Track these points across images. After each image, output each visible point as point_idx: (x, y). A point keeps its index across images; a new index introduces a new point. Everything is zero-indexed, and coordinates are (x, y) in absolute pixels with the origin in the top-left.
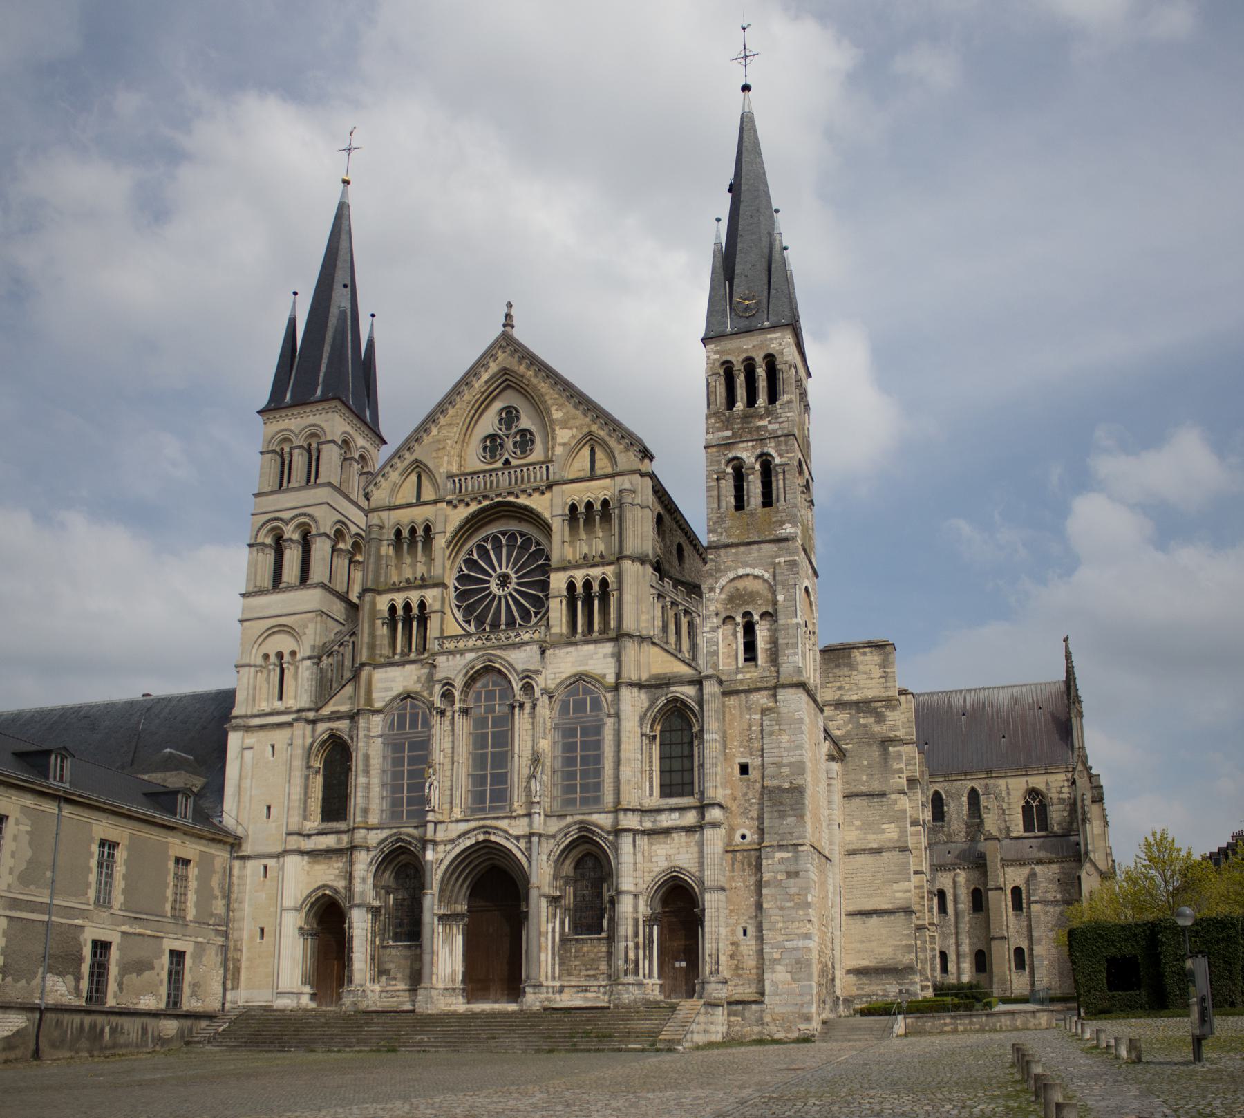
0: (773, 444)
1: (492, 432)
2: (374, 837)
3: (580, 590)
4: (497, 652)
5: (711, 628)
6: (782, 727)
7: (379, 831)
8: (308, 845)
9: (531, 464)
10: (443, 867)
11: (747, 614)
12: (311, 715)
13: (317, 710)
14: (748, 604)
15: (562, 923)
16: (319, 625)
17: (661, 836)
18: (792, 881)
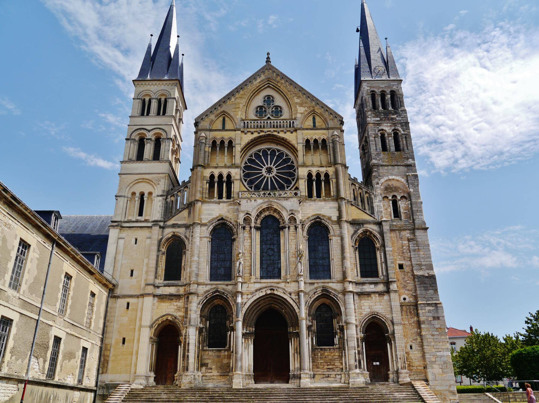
0: (399, 126)
1: (261, 104)
2: (202, 290)
3: (314, 178)
4: (275, 200)
5: (379, 200)
6: (419, 248)
7: (204, 286)
8: (159, 291)
9: (282, 120)
10: (246, 306)
11: (394, 196)
12: (162, 224)
13: (165, 222)
14: (395, 192)
15: (312, 339)
16: (166, 181)
17: (366, 296)
18: (436, 321)
